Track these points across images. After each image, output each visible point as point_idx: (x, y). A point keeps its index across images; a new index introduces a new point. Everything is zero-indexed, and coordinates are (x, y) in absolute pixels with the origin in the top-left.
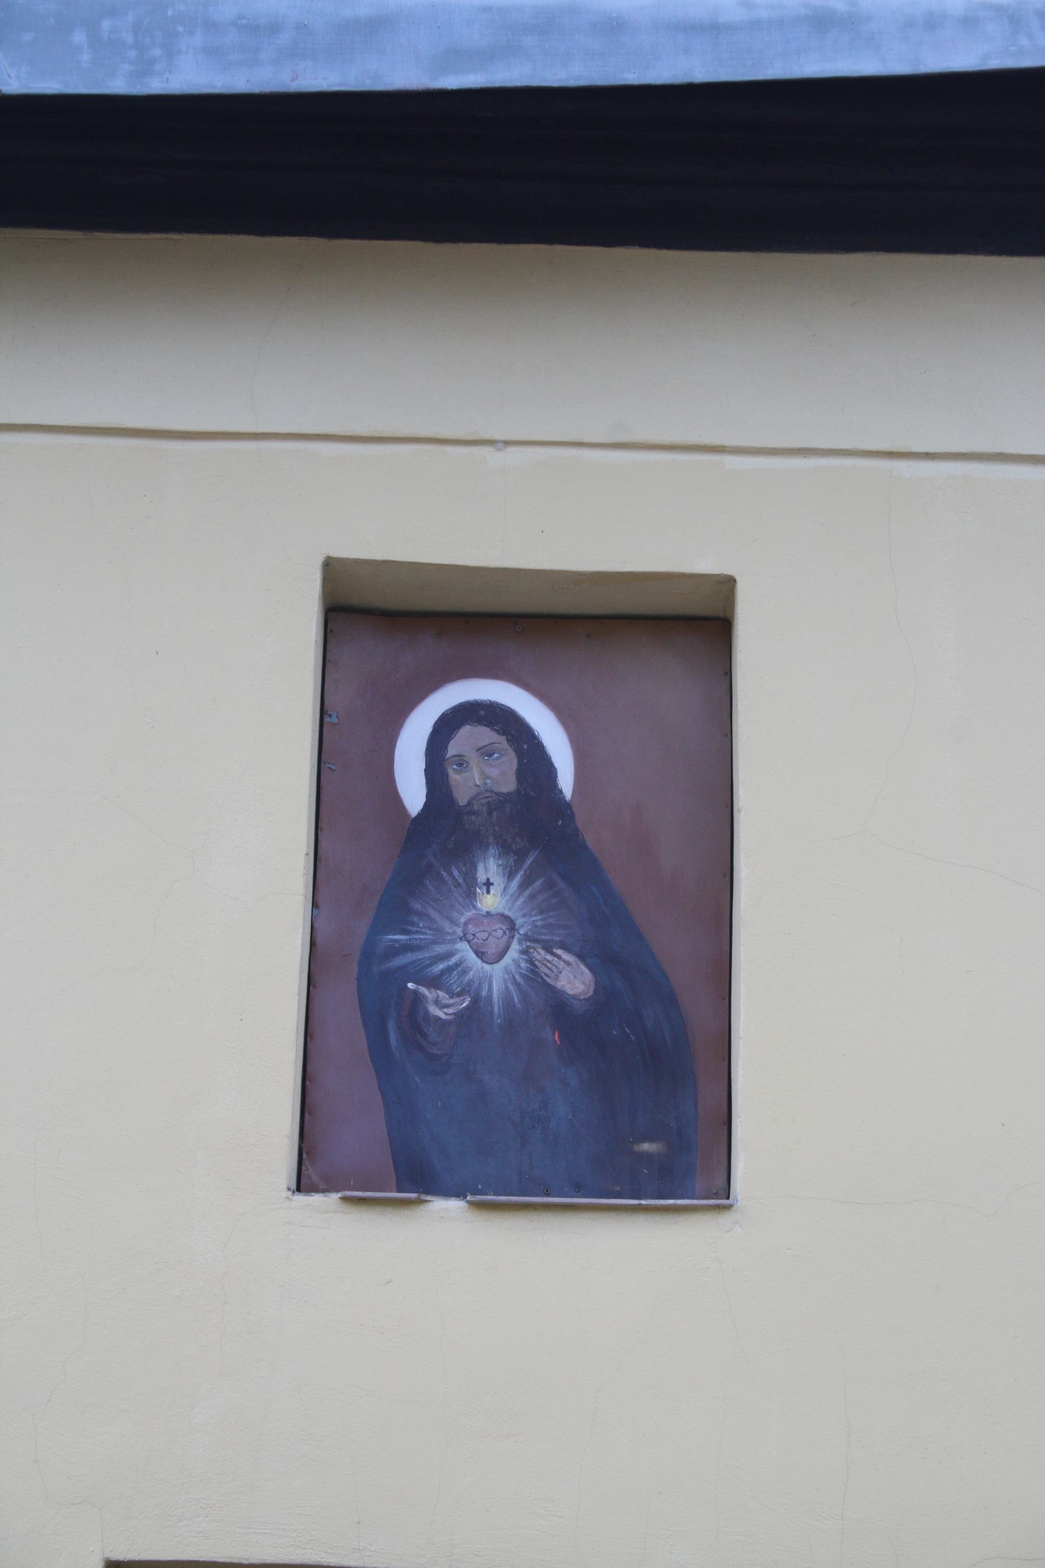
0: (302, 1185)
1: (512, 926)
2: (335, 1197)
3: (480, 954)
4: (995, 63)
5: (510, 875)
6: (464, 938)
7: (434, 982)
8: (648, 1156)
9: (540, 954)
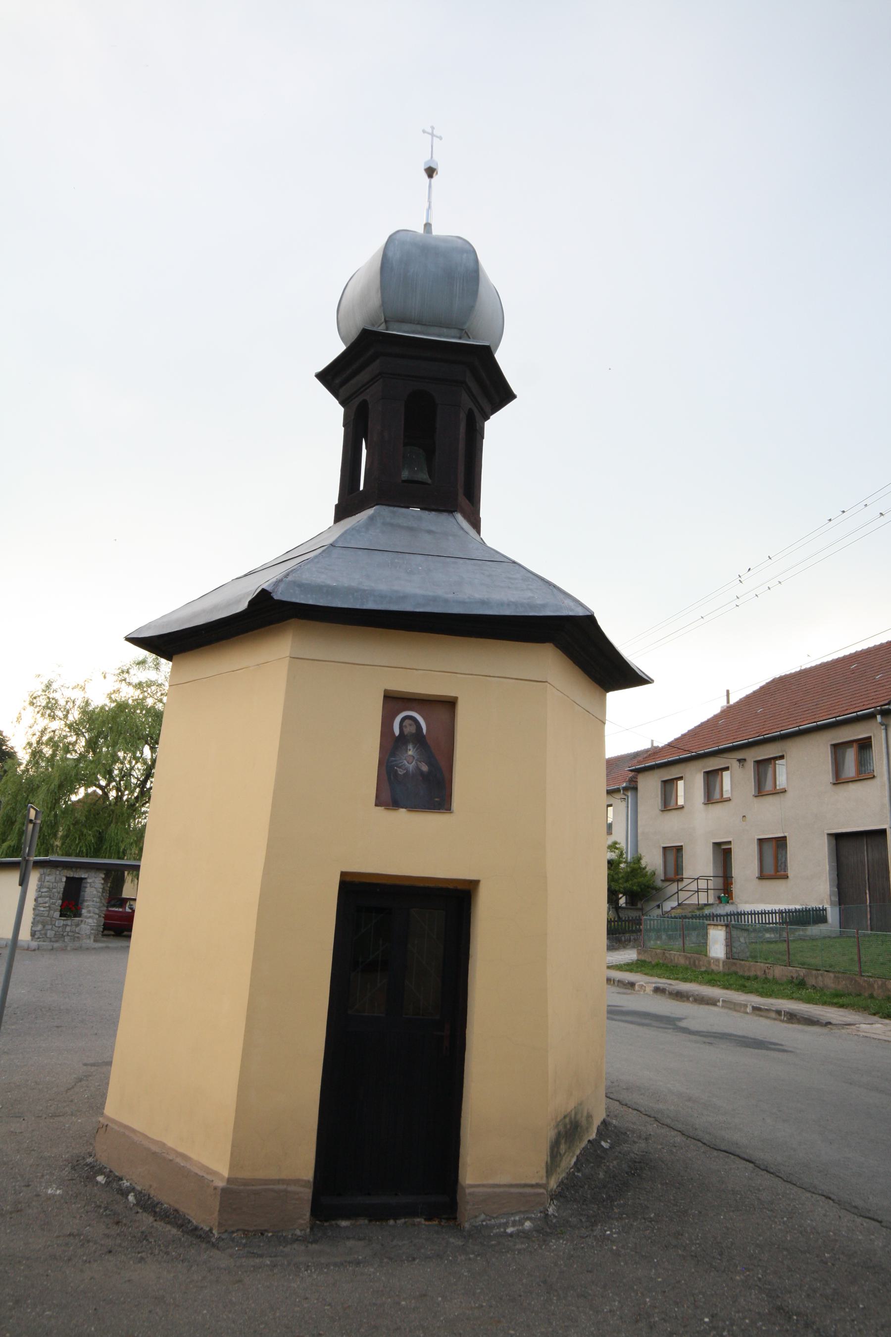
0: (376, 805)
1: (414, 757)
2: (383, 808)
3: (408, 762)
4: (513, 614)
5: (414, 748)
6: (405, 759)
7: (400, 767)
8: (437, 801)
9: (419, 763)
